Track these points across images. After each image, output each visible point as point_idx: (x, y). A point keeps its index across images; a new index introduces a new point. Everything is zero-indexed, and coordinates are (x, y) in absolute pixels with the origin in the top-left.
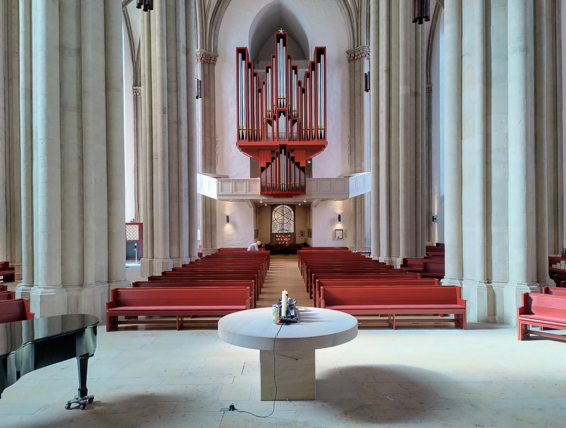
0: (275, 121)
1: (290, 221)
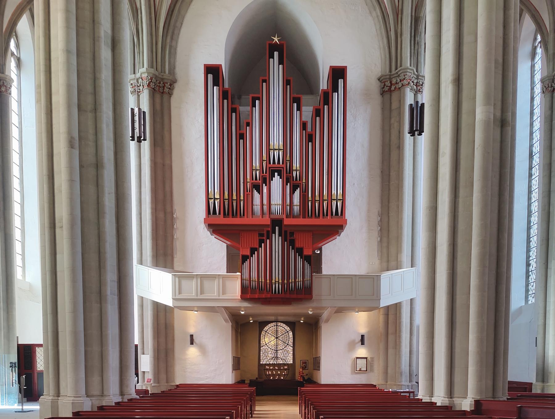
0: (266, 185)
1: (287, 347)
